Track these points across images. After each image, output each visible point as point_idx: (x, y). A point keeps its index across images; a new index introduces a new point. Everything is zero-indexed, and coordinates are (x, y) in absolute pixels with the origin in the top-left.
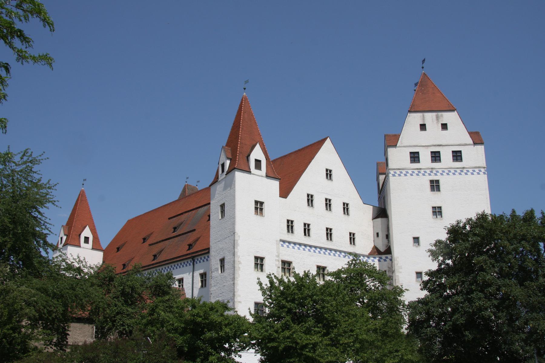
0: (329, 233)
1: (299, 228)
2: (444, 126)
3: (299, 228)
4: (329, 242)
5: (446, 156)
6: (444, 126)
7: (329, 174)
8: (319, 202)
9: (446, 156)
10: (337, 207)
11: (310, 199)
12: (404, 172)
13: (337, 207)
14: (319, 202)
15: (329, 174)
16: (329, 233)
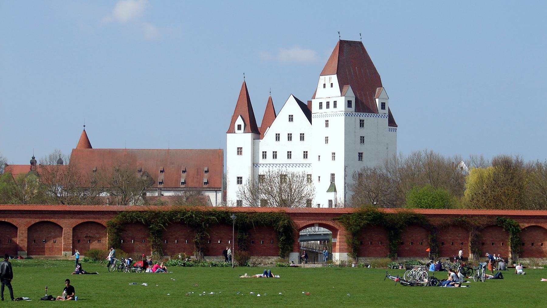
0: (289, 155)
1: (270, 155)
2: (332, 85)
3: (270, 155)
4: (289, 160)
5: (331, 105)
6: (332, 85)
7: (291, 118)
8: (284, 137)
9: (331, 105)
10: (296, 137)
11: (278, 137)
12: (316, 114)
13: (296, 137)
14: (284, 137)
15: (291, 118)
16: (289, 155)
